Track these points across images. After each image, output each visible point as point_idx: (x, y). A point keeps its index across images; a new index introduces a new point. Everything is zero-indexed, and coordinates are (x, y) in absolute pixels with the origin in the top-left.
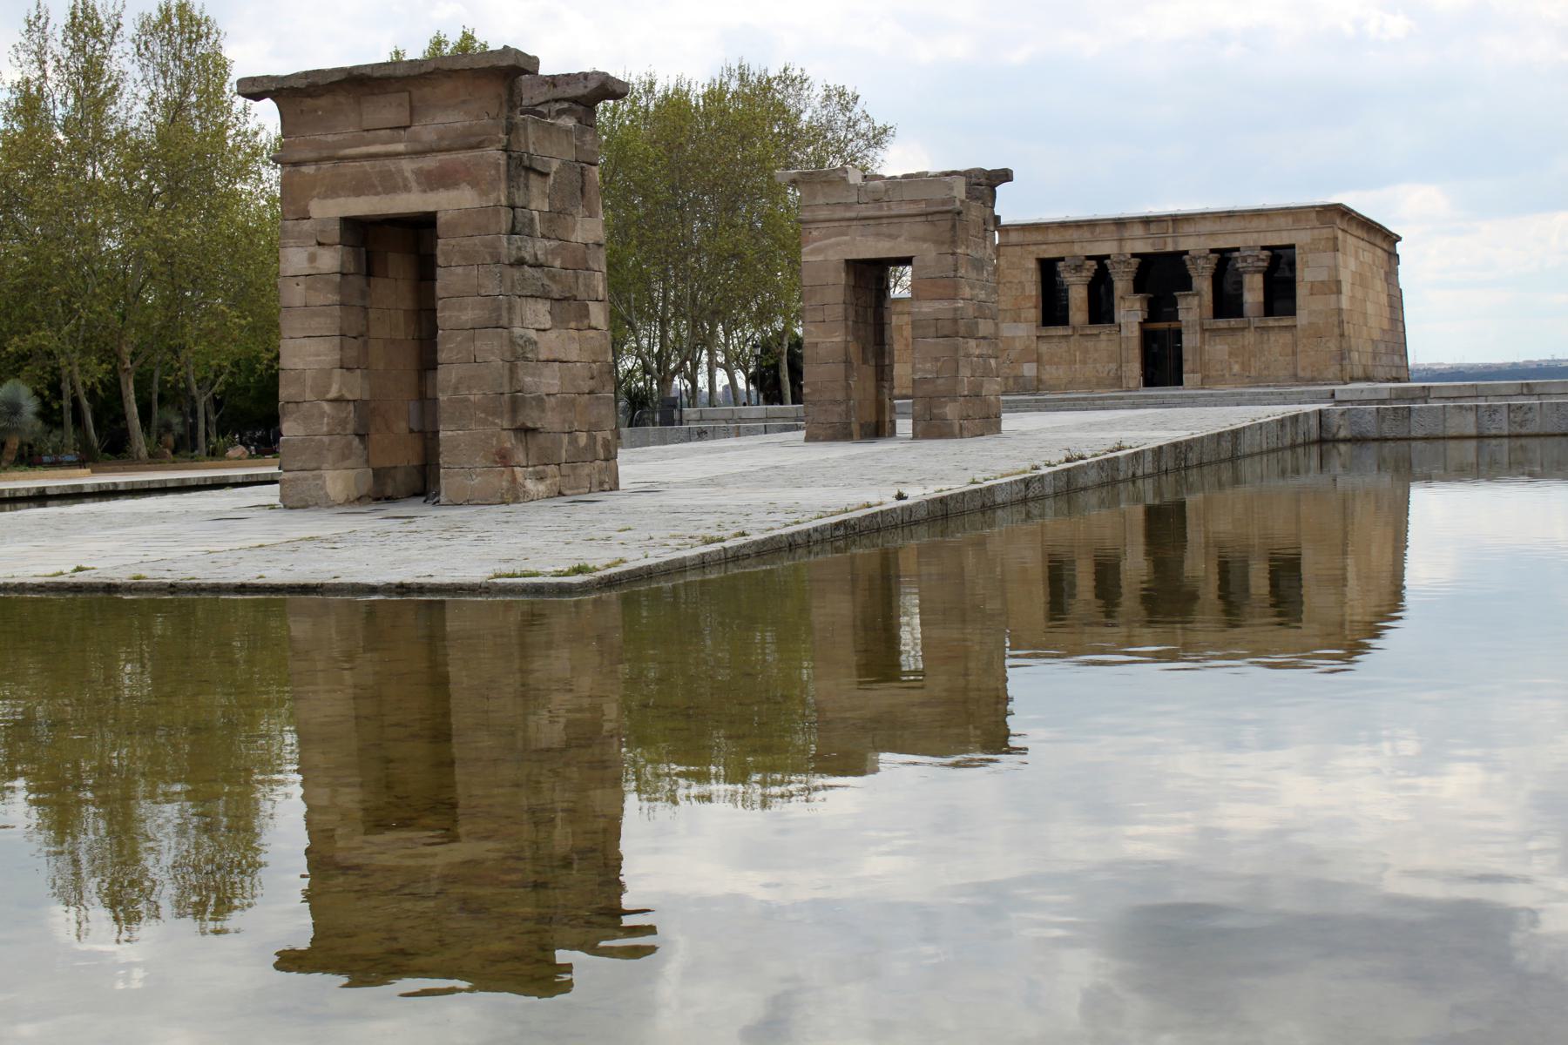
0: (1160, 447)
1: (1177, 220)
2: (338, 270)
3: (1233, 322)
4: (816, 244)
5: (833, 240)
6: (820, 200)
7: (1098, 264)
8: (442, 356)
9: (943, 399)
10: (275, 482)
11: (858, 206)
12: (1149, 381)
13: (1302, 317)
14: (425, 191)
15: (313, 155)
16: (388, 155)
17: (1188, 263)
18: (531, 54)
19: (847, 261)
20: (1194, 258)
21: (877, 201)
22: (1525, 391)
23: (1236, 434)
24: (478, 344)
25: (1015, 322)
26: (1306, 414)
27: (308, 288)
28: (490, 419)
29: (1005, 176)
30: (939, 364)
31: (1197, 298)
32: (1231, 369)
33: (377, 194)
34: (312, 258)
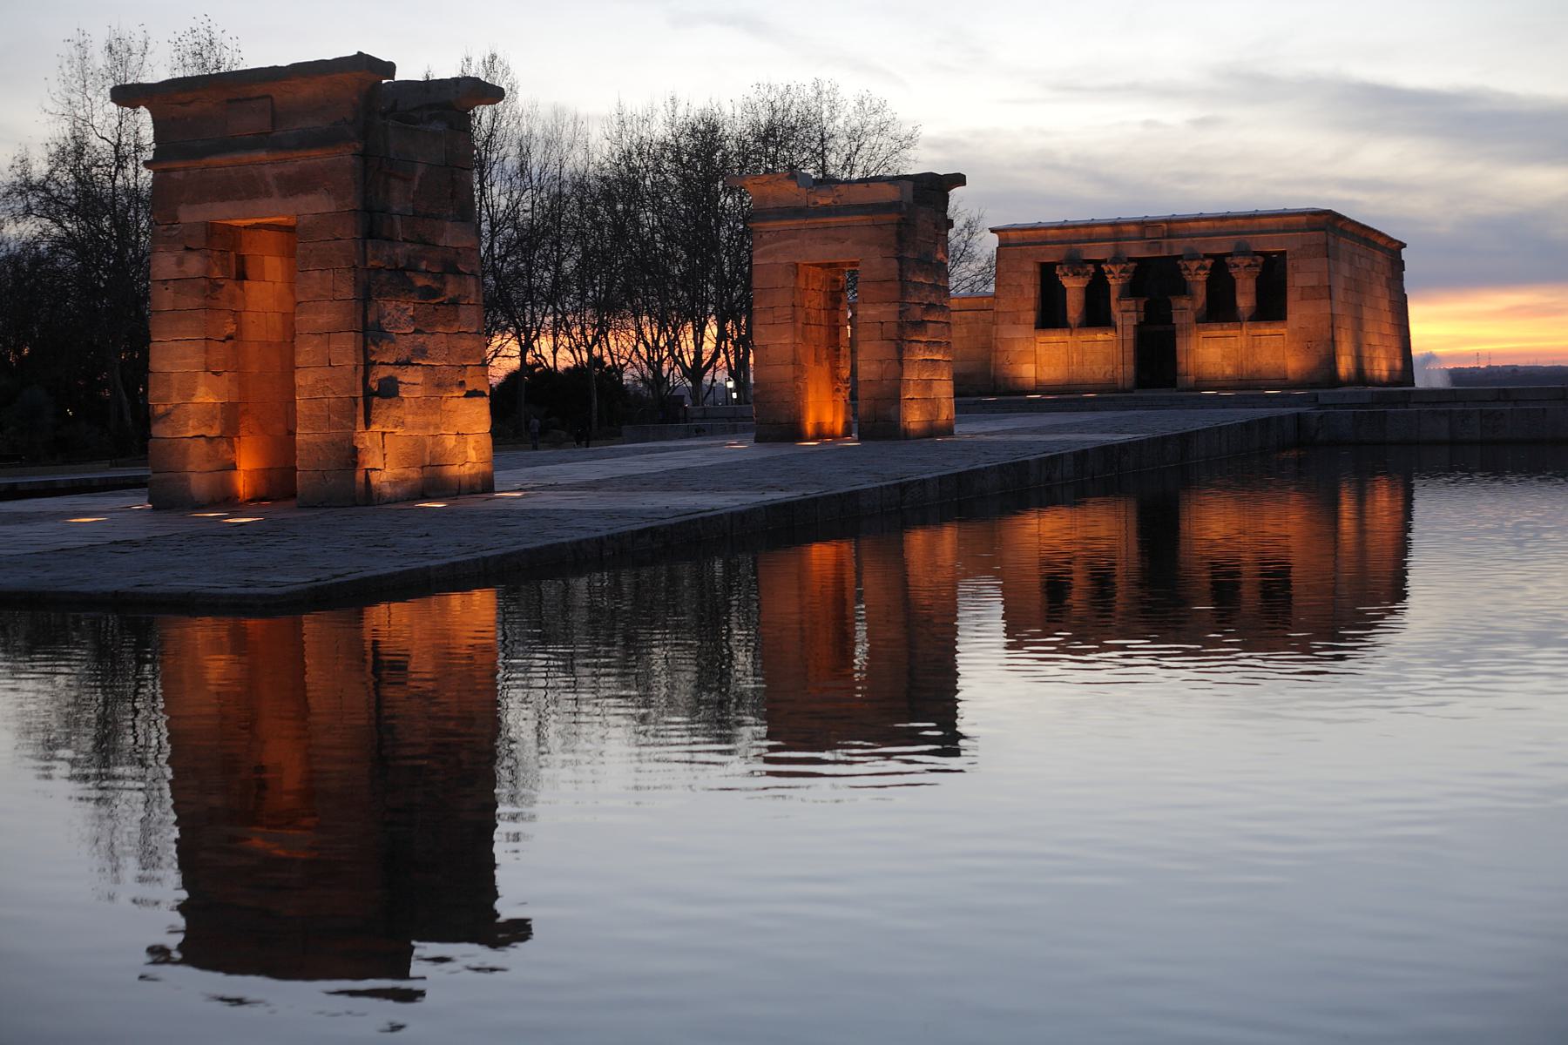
0: (1085, 452)
4: (766, 247)
5: (783, 243)
7: (1095, 267)
8: (300, 360)
10: (144, 485)
14: (284, 196)
18: (386, 59)
23: (1185, 439)
25: (1014, 323)
26: (1281, 418)
27: (176, 292)
28: (344, 422)
29: (959, 180)
30: (884, 366)
33: (240, 199)
34: (180, 263)
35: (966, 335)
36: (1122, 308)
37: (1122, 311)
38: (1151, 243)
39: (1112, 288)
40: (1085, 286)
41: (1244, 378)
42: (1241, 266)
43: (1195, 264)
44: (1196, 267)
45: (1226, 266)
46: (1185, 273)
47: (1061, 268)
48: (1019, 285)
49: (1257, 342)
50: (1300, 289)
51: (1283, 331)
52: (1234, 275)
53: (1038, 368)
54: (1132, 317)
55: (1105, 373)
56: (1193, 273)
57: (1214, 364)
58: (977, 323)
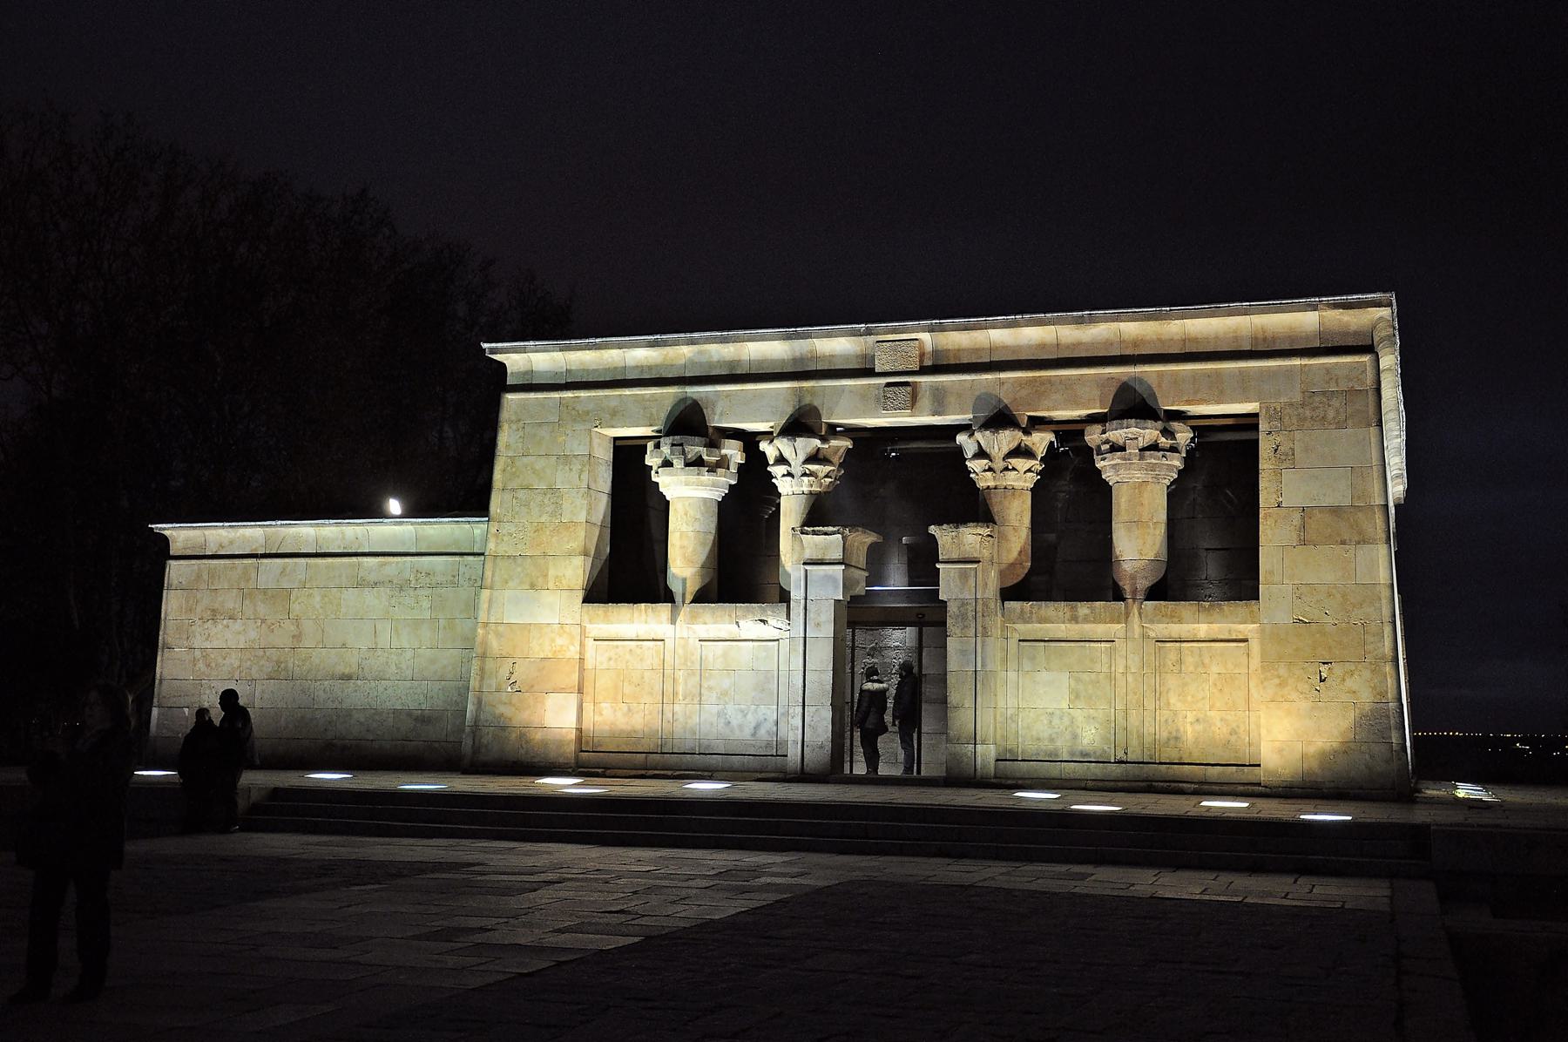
25: (533, 586)
35: (427, 615)
36: (808, 555)
37: (804, 564)
38: (889, 385)
39: (784, 503)
40: (718, 494)
41: (1131, 757)
42: (1132, 451)
43: (1006, 439)
44: (1005, 450)
45: (1087, 453)
46: (975, 466)
47: (657, 446)
48: (552, 490)
49: (1173, 656)
50: (1297, 517)
51: (1248, 629)
52: (1109, 476)
53: (588, 707)
54: (830, 578)
55: (757, 727)
56: (999, 465)
57: (1052, 714)
58: (456, 585)
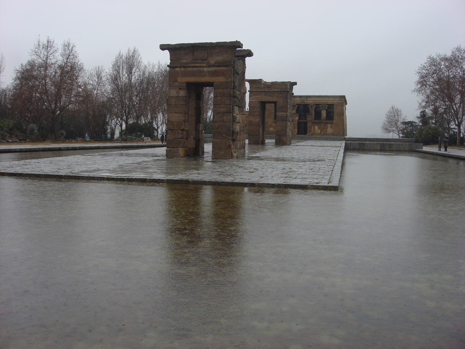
1: (307, 97)
2: (185, 96)
3: (319, 121)
5: (257, 96)
6: (254, 86)
9: (283, 136)
11: (264, 88)
12: (298, 133)
13: (334, 121)
15: (179, 65)
16: (200, 67)
17: (309, 107)
19: (260, 101)
20: (311, 106)
21: (268, 87)
22: (387, 140)
24: (224, 117)
28: (227, 137)
29: (295, 84)
31: (311, 115)
32: (318, 132)
34: (178, 92)
